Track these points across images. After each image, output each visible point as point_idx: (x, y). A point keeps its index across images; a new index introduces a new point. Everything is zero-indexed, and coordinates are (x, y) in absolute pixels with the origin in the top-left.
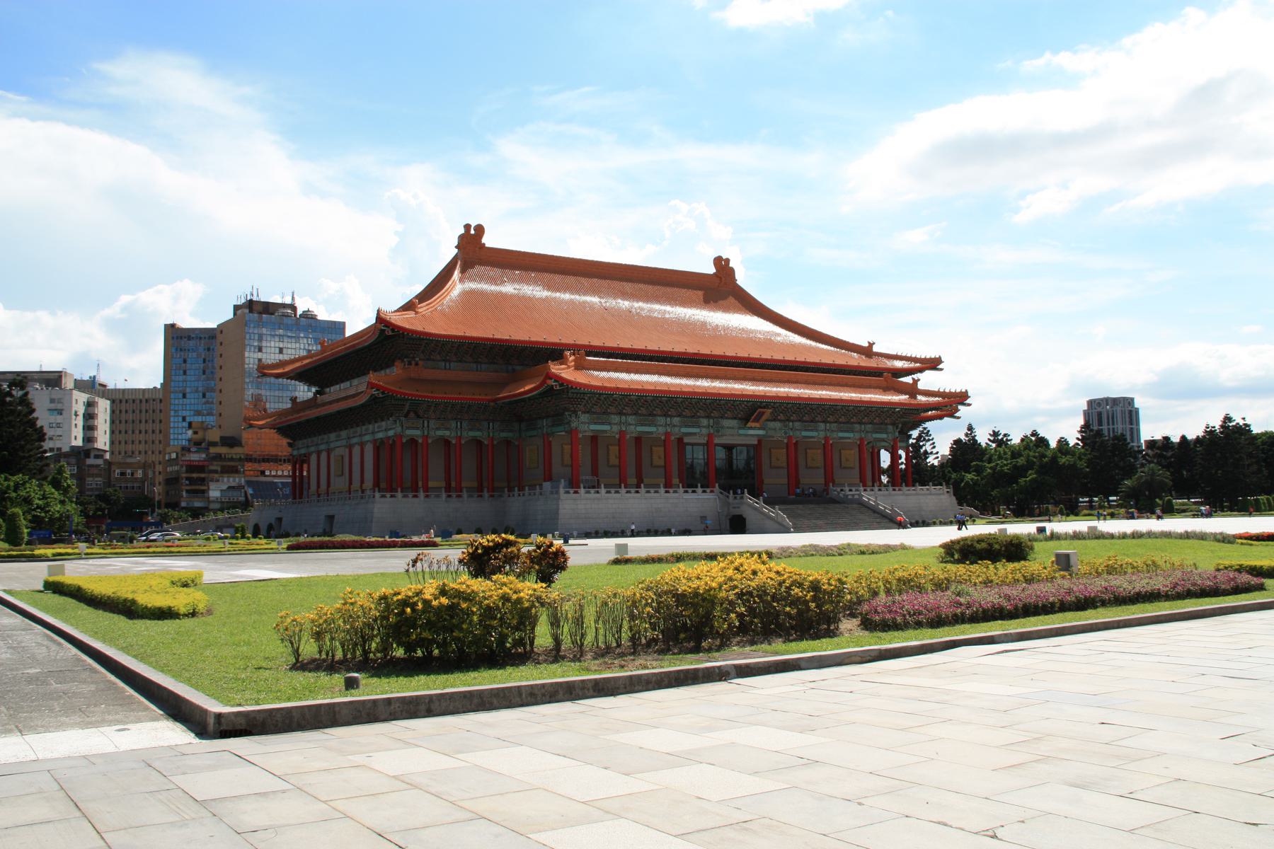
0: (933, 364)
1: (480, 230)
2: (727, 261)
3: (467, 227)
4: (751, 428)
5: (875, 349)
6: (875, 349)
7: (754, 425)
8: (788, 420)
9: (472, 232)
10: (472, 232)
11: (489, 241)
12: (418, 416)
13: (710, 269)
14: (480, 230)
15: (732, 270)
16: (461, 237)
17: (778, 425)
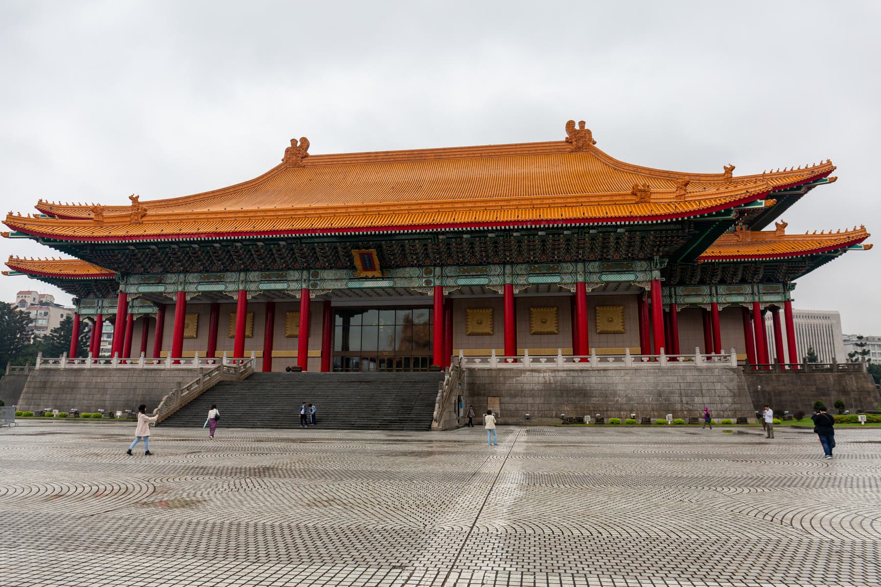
0: (820, 176)
1: (305, 142)
2: (582, 124)
3: (294, 141)
4: (366, 278)
5: (735, 174)
6: (735, 174)
7: (370, 274)
8: (435, 266)
9: (299, 144)
10: (299, 144)
11: (311, 152)
12: (97, 297)
13: (562, 135)
14: (304, 140)
15: (589, 132)
16: (287, 150)
17: (415, 271)
